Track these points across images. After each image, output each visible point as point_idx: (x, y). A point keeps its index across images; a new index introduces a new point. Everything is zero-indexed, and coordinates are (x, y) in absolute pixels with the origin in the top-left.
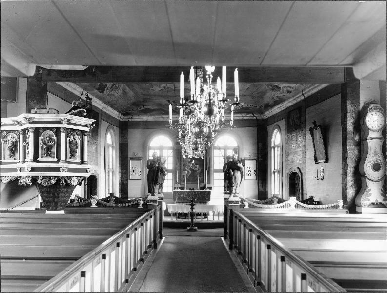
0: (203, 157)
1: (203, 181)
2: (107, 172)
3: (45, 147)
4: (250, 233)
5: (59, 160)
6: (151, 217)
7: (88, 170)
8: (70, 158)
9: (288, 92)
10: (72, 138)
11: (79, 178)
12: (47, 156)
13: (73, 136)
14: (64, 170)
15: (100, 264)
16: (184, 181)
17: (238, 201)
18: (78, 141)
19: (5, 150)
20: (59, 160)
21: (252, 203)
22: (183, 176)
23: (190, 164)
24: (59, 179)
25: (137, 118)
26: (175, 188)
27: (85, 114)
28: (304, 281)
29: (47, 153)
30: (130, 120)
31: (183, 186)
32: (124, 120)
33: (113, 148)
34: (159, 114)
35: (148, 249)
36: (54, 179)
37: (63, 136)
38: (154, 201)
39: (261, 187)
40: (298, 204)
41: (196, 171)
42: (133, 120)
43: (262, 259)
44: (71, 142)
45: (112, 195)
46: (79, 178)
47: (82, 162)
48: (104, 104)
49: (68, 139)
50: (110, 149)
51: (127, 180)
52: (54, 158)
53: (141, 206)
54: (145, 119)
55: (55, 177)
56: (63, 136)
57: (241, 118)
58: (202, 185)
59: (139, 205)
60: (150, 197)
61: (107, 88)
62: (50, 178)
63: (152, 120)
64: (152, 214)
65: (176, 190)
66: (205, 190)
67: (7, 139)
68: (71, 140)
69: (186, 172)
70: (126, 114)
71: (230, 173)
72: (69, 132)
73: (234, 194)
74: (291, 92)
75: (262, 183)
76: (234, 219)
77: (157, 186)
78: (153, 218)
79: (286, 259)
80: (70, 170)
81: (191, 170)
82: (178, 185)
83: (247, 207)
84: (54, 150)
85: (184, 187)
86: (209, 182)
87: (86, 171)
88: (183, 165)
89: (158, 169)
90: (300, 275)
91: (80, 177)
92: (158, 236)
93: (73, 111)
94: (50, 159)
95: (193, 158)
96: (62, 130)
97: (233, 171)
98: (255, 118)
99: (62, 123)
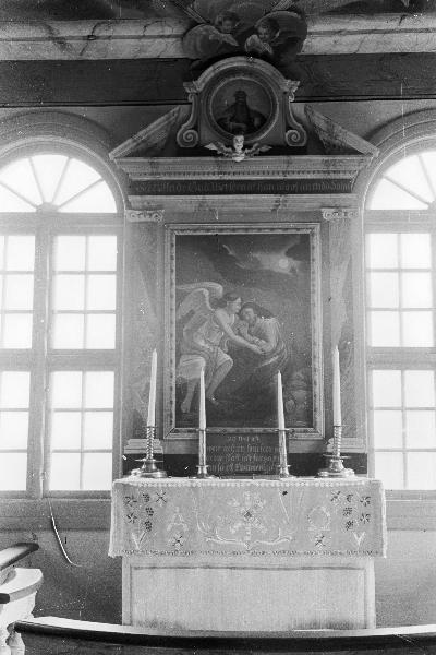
23: (220, 313)
26: (129, 464)
31: (181, 449)
41: (264, 357)
66: (323, 481)
69: (202, 362)
81: (237, 352)
82: (153, 446)
88: (180, 324)
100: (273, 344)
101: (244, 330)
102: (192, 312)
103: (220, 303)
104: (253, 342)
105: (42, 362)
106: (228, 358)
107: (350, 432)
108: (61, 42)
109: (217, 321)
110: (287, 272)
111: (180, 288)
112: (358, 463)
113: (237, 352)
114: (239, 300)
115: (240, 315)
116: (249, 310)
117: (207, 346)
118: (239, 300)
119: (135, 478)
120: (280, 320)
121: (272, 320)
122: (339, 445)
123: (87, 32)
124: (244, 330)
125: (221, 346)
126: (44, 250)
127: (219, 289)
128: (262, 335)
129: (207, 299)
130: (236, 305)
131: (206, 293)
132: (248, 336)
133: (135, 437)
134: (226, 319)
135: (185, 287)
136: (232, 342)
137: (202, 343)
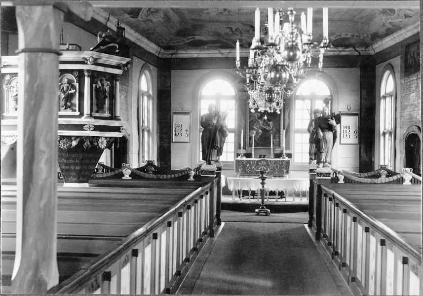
0: (280, 110)
1: (279, 145)
2: (141, 130)
3: (63, 96)
4: (344, 214)
5: (82, 115)
6: (207, 193)
7: (121, 128)
8: (97, 112)
9: (406, 16)
10: (99, 84)
11: (108, 139)
12: (66, 109)
13: (101, 81)
14: (90, 128)
15: (151, 244)
16: (250, 145)
17: (330, 174)
18: (107, 88)
19: (8, 100)
20: (82, 115)
21: (349, 176)
22: (250, 138)
23: (259, 121)
24: (82, 140)
25: (184, 54)
27: (117, 51)
28: (406, 265)
29: (66, 104)
30: (174, 56)
31: (250, 152)
32: (165, 56)
33: (149, 96)
34: (216, 48)
35: (202, 237)
36: (75, 140)
37: (87, 80)
38: (210, 172)
39: (364, 155)
40: (415, 179)
42: (178, 56)
43: (359, 247)
44: (97, 90)
45: (150, 163)
46: (108, 139)
47: (113, 117)
48: (137, 34)
49: (94, 85)
50: (146, 98)
51: (169, 142)
52: (75, 111)
53: (192, 179)
54: (195, 56)
55: (77, 137)
56: (87, 80)
57: (336, 53)
58: (278, 151)
59: (188, 176)
60: (205, 166)
61: (142, 11)
62: (69, 138)
63: (207, 56)
64: (208, 190)
65: (239, 158)
66: (281, 159)
67: (12, 85)
68: (98, 87)
69: (255, 132)
70: (167, 48)
71: (317, 133)
72: (94, 76)
73: (324, 163)
74: (410, 17)
75: (366, 149)
76: (323, 198)
77: (215, 151)
78: (209, 196)
79: (387, 242)
80: (97, 128)
81: (264, 130)
82: (242, 151)
83: (341, 181)
84: (76, 101)
86: (288, 147)
87: (117, 129)
88: (250, 123)
89: (216, 128)
90: (402, 260)
91: (110, 138)
92: (215, 220)
93: (102, 47)
94: (69, 112)
95: (266, 112)
96: (86, 74)
97: (323, 131)
98: (357, 53)
99: (86, 64)
101: (265, 125)
106: (261, 131)
108: (222, 54)
112: (290, 156)
113: (264, 130)
119: (239, 158)
121: (271, 122)
122: (285, 152)
123: (229, 52)
124: (265, 125)
128: (269, 125)
136: (262, 127)
137: (255, 128)
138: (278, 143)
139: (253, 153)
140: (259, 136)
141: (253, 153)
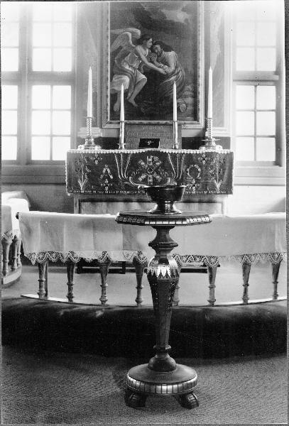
16: (115, 116)
22: (115, 97)
23: (139, 48)
31: (113, 134)
41: (167, 76)
58: (191, 130)
65: (81, 149)
66: (203, 150)
69: (127, 79)
81: (150, 74)
85: (118, 139)
88: (114, 54)
100: (173, 68)
102: (121, 48)
103: (139, 42)
104: (160, 67)
105: (26, 76)
106: (144, 77)
107: (220, 123)
109: (138, 54)
110: (182, 21)
111: (113, 31)
112: (225, 142)
113: (150, 74)
114: (151, 40)
115: (152, 49)
116: (158, 46)
117: (130, 69)
118: (151, 40)
120: (175, 51)
122: (213, 133)
125: (139, 69)
126: (52, 112)
127: (139, 32)
128: (166, 63)
129: (131, 38)
130: (149, 43)
131: (130, 35)
132: (155, 62)
133: (83, 126)
134: (143, 52)
135: (118, 31)
136: (146, 67)
137: (127, 67)
138: (190, 108)
139: (122, 136)
140: (137, 91)
141: (122, 136)
